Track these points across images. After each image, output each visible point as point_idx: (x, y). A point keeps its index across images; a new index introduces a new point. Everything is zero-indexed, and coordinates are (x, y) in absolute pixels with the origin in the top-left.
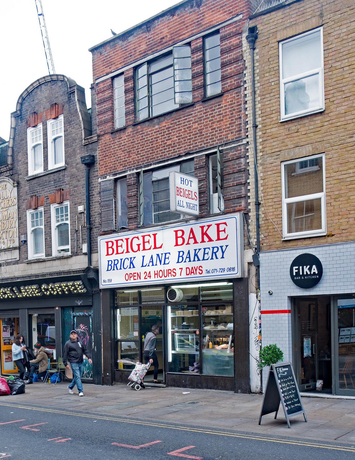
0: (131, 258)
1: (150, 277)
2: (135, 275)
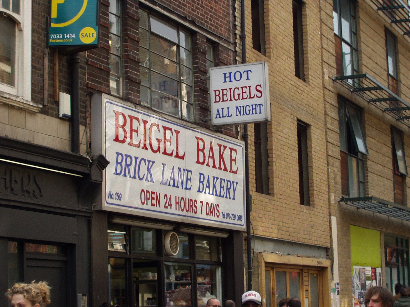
1: (171, 205)
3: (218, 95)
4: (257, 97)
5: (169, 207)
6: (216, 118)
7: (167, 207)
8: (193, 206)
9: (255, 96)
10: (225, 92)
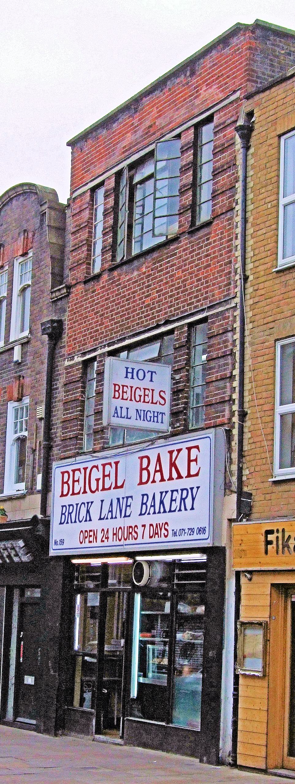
0: (88, 503)
1: (107, 538)
5: (106, 540)
8: (133, 533)
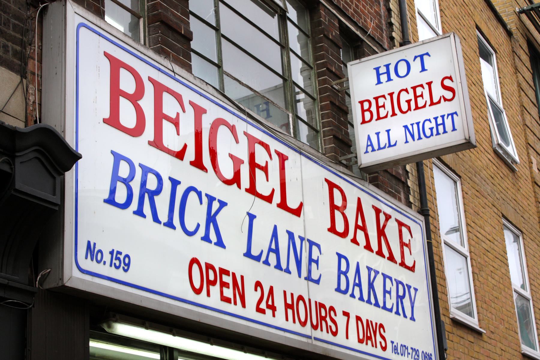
0: (211, 199)
1: (273, 308)
2: (226, 278)
3: (369, 110)
4: (445, 100)
5: (269, 312)
6: (367, 152)
7: (263, 311)
8: (328, 319)
9: (442, 100)
10: (381, 101)
